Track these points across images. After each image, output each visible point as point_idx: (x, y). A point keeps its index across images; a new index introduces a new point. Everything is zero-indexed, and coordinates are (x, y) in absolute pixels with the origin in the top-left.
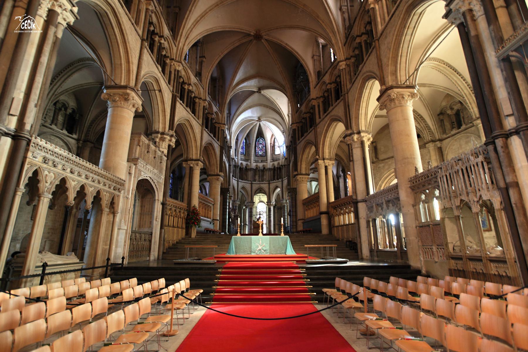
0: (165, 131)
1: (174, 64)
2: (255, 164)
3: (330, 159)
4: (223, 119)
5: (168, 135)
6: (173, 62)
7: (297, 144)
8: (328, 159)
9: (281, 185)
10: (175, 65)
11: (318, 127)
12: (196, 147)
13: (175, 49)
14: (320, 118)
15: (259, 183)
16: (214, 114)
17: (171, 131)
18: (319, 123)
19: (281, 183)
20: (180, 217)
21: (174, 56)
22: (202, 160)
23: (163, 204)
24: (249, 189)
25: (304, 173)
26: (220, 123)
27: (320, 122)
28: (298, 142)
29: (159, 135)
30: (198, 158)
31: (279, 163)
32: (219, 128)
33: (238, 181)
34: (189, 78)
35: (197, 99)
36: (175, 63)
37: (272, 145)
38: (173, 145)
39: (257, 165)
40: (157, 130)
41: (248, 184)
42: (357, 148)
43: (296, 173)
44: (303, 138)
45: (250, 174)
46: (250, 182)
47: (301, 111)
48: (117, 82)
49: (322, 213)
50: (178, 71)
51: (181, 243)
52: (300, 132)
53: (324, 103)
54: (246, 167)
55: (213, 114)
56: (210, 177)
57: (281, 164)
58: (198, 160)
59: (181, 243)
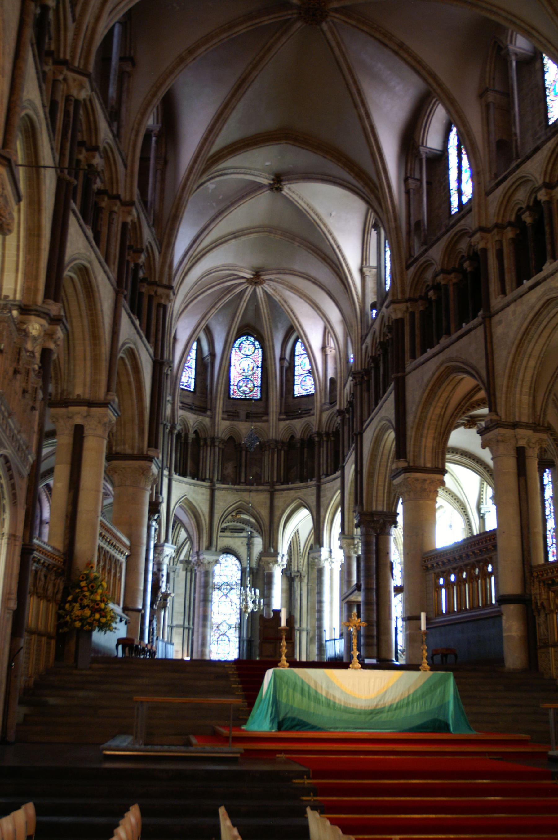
1: (65, 79)
2: (227, 423)
6: (65, 72)
7: (408, 369)
8: (527, 426)
9: (314, 498)
10: (70, 81)
11: (496, 319)
14: (503, 292)
17: (51, 302)
19: (314, 490)
21: (68, 50)
22: (116, 406)
24: (203, 508)
25: (429, 465)
27: (508, 305)
31: (308, 426)
32: (151, 298)
35: (106, 199)
36: (71, 75)
37: (286, 364)
47: (428, 265)
50: (77, 102)
52: (417, 332)
57: (315, 429)
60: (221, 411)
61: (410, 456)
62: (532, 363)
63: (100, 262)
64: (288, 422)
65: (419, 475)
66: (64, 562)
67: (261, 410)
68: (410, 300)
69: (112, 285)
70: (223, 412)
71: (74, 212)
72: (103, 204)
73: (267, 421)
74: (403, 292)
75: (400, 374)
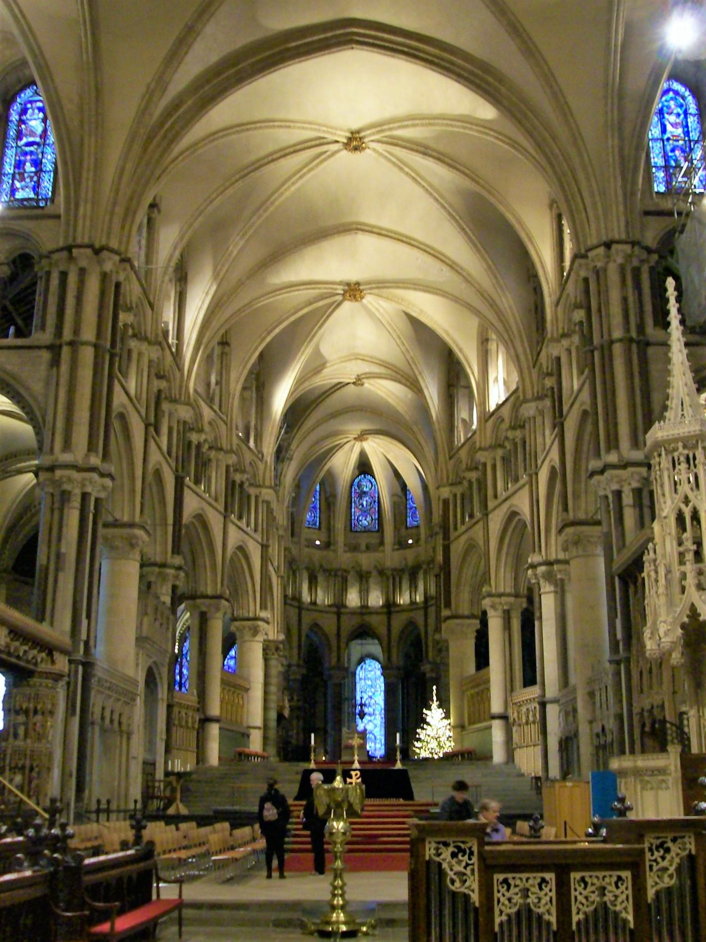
0: (166, 559)
2: (349, 555)
7: (452, 538)
8: (509, 595)
11: (490, 516)
13: (178, 374)
14: (496, 496)
17: (176, 556)
20: (187, 727)
23: (170, 707)
25: (466, 613)
28: (453, 535)
29: (157, 569)
30: (218, 592)
32: (257, 497)
34: (199, 416)
40: (153, 560)
42: (548, 593)
43: (445, 613)
48: (118, 516)
56: (237, 623)
60: (342, 545)
62: (512, 551)
63: (210, 504)
64: (401, 552)
66: (199, 703)
68: (452, 485)
69: (220, 513)
70: (345, 545)
71: (189, 487)
75: (446, 542)
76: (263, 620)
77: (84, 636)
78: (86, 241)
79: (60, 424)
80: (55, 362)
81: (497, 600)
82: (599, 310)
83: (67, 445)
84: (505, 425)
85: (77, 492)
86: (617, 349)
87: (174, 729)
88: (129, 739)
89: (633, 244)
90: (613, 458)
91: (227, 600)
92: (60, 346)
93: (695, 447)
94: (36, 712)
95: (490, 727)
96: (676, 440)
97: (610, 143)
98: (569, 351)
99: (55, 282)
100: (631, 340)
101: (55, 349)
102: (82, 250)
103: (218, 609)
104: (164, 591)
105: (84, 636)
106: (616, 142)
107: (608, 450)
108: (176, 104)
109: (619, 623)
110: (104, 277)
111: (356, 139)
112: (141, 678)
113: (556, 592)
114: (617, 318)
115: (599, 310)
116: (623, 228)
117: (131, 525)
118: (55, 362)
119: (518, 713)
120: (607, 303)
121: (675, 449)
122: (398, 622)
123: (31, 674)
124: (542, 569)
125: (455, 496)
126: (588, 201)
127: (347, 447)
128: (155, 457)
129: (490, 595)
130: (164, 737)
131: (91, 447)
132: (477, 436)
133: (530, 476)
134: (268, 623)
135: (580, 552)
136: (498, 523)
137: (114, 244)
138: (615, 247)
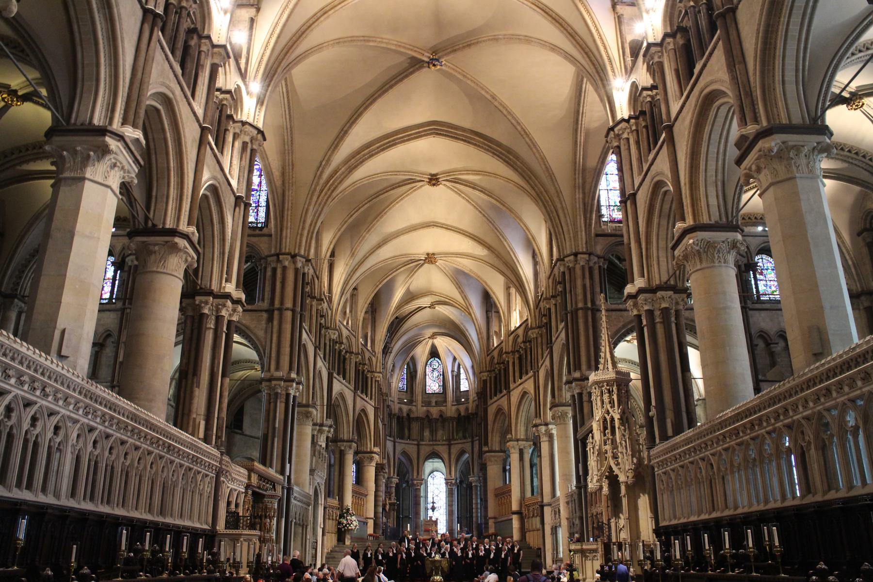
2: (425, 408)
3: (527, 440)
4: (378, 364)
5: (326, 426)
7: (489, 404)
8: (523, 440)
9: (470, 448)
11: (511, 393)
12: (348, 422)
13: (330, 312)
14: (515, 382)
15: (431, 443)
16: (367, 362)
18: (514, 389)
19: (470, 444)
23: (325, 508)
25: (497, 449)
26: (373, 372)
28: (490, 402)
31: (467, 409)
32: (372, 378)
33: (394, 442)
36: (330, 331)
37: (455, 373)
38: (330, 435)
39: (428, 411)
41: (411, 446)
43: (485, 449)
44: (495, 398)
45: (415, 427)
46: (415, 442)
49: (514, 513)
51: (336, 551)
52: (493, 386)
53: (520, 358)
54: (408, 415)
55: (365, 364)
56: (360, 455)
57: (470, 412)
58: (352, 441)
59: (336, 551)
61: (490, 444)
62: (524, 414)
65: (493, 454)
67: (443, 400)
68: (489, 371)
70: (422, 402)
72: (347, 357)
73: (446, 406)
74: (486, 367)
76: (375, 453)
77: (288, 474)
78: (287, 251)
79: (274, 355)
80: (270, 319)
81: (516, 443)
82: (571, 291)
83: (278, 368)
84: (520, 340)
85: (284, 392)
86: (580, 313)
87: (327, 520)
88: (306, 528)
89: (590, 254)
90: (577, 375)
91: (355, 442)
92: (273, 311)
93: (613, 385)
94: (266, 517)
95: (512, 519)
96: (603, 382)
97: (577, 196)
98: (555, 305)
99: (269, 273)
100: (588, 309)
101: (270, 312)
102: (285, 256)
103: (350, 447)
104: (322, 440)
105: (288, 474)
106: (581, 196)
107: (575, 371)
108: (335, 172)
109: (580, 465)
110: (297, 270)
111: (434, 179)
112: (312, 492)
113: (549, 441)
114: (580, 297)
115: (571, 291)
116: (584, 246)
117: (307, 406)
118: (270, 319)
119: (528, 510)
120: (575, 287)
121: (603, 386)
122: (455, 450)
123: (263, 496)
124: (543, 429)
125: (491, 378)
126: (565, 229)
127: (424, 342)
128: (320, 363)
129: (511, 440)
130: (322, 526)
131: (291, 369)
132: (504, 344)
133: (535, 373)
134: (378, 454)
135: (562, 422)
136: (516, 398)
137: (302, 253)
138: (579, 256)
